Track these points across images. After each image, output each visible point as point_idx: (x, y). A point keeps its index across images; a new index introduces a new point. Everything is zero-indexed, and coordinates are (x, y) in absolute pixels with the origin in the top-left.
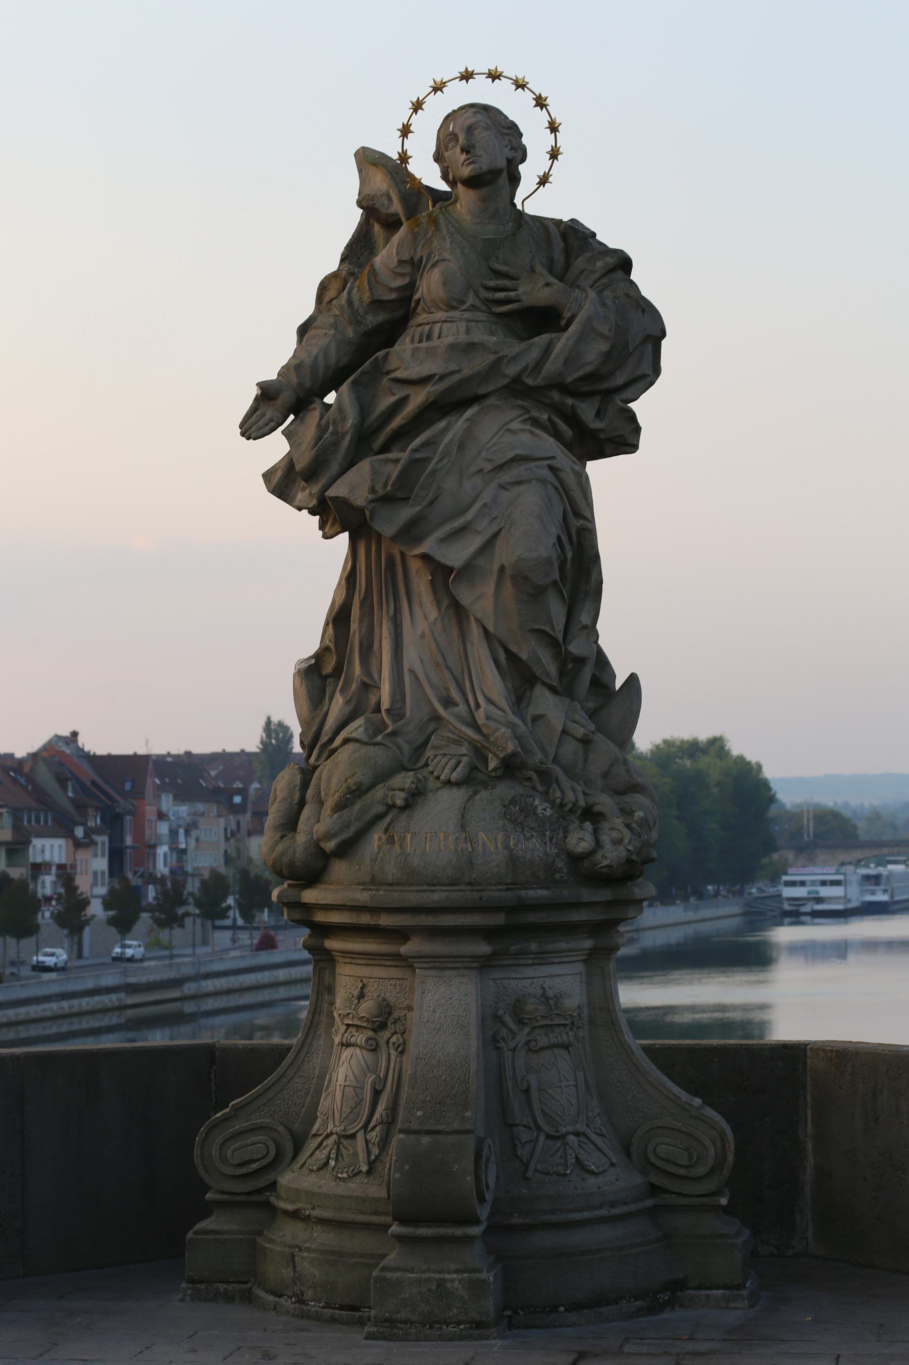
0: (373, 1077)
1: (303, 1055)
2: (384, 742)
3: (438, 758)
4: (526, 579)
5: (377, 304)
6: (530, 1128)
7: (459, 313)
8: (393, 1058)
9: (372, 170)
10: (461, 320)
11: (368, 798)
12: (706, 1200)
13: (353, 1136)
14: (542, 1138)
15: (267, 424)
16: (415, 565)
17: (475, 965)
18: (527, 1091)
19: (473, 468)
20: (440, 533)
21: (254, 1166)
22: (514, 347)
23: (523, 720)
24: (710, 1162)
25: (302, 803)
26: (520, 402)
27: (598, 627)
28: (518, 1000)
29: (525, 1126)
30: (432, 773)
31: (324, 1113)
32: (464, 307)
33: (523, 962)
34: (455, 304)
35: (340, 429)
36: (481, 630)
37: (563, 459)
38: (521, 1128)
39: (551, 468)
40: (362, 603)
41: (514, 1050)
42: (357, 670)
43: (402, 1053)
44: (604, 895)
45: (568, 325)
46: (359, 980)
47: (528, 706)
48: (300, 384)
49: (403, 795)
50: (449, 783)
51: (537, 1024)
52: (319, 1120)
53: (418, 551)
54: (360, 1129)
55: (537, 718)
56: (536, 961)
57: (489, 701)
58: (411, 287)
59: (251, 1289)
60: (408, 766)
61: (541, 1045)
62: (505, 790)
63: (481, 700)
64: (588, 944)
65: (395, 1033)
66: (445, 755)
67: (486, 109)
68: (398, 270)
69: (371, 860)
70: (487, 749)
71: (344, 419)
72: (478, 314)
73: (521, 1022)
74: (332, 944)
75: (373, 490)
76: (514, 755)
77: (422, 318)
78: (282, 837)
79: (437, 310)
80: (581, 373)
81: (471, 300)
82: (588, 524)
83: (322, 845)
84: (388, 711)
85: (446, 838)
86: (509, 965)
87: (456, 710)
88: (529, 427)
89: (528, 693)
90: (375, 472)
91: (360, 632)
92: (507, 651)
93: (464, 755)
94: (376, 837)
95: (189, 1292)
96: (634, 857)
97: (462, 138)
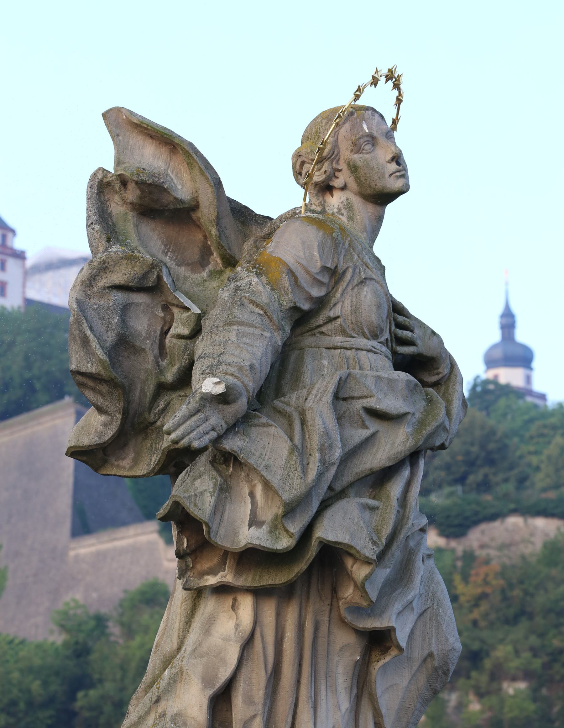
7: (377, 343)
15: (208, 433)
35: (327, 459)
68: (319, 277)
79: (358, 335)
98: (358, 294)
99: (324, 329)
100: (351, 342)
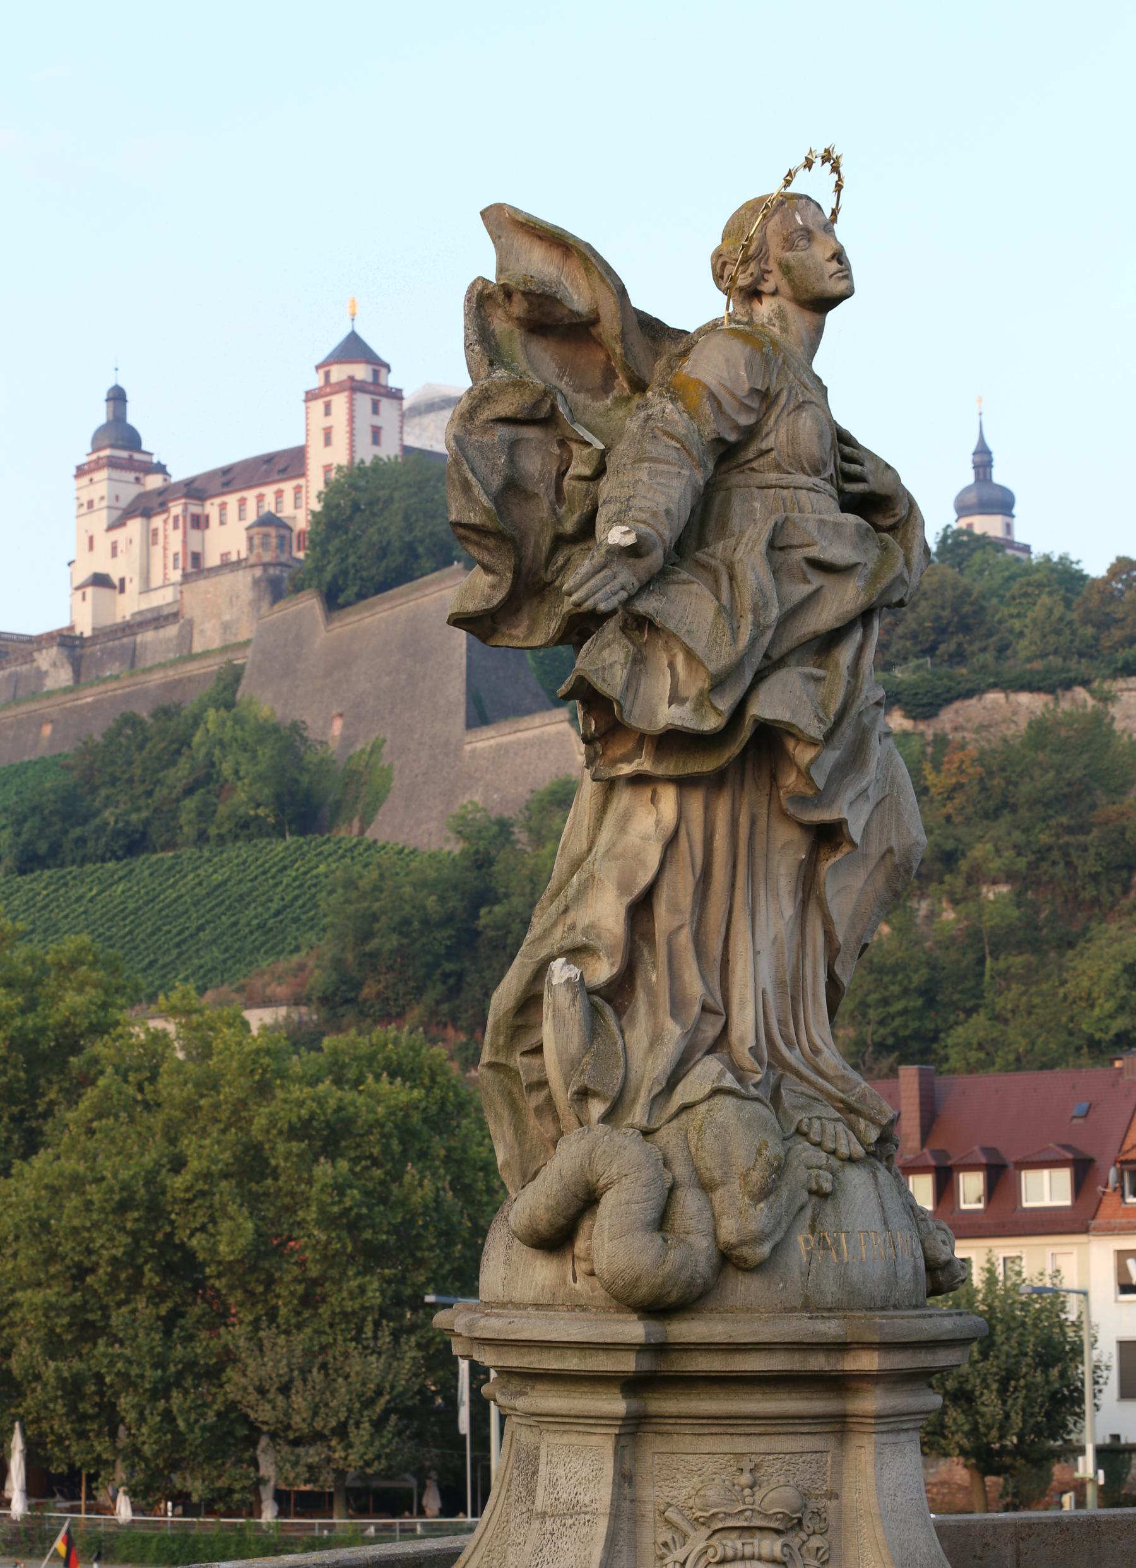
9: (522, 243)
15: (616, 593)
69: (802, 1274)
98: (795, 421)
99: (754, 465)
100: (787, 479)
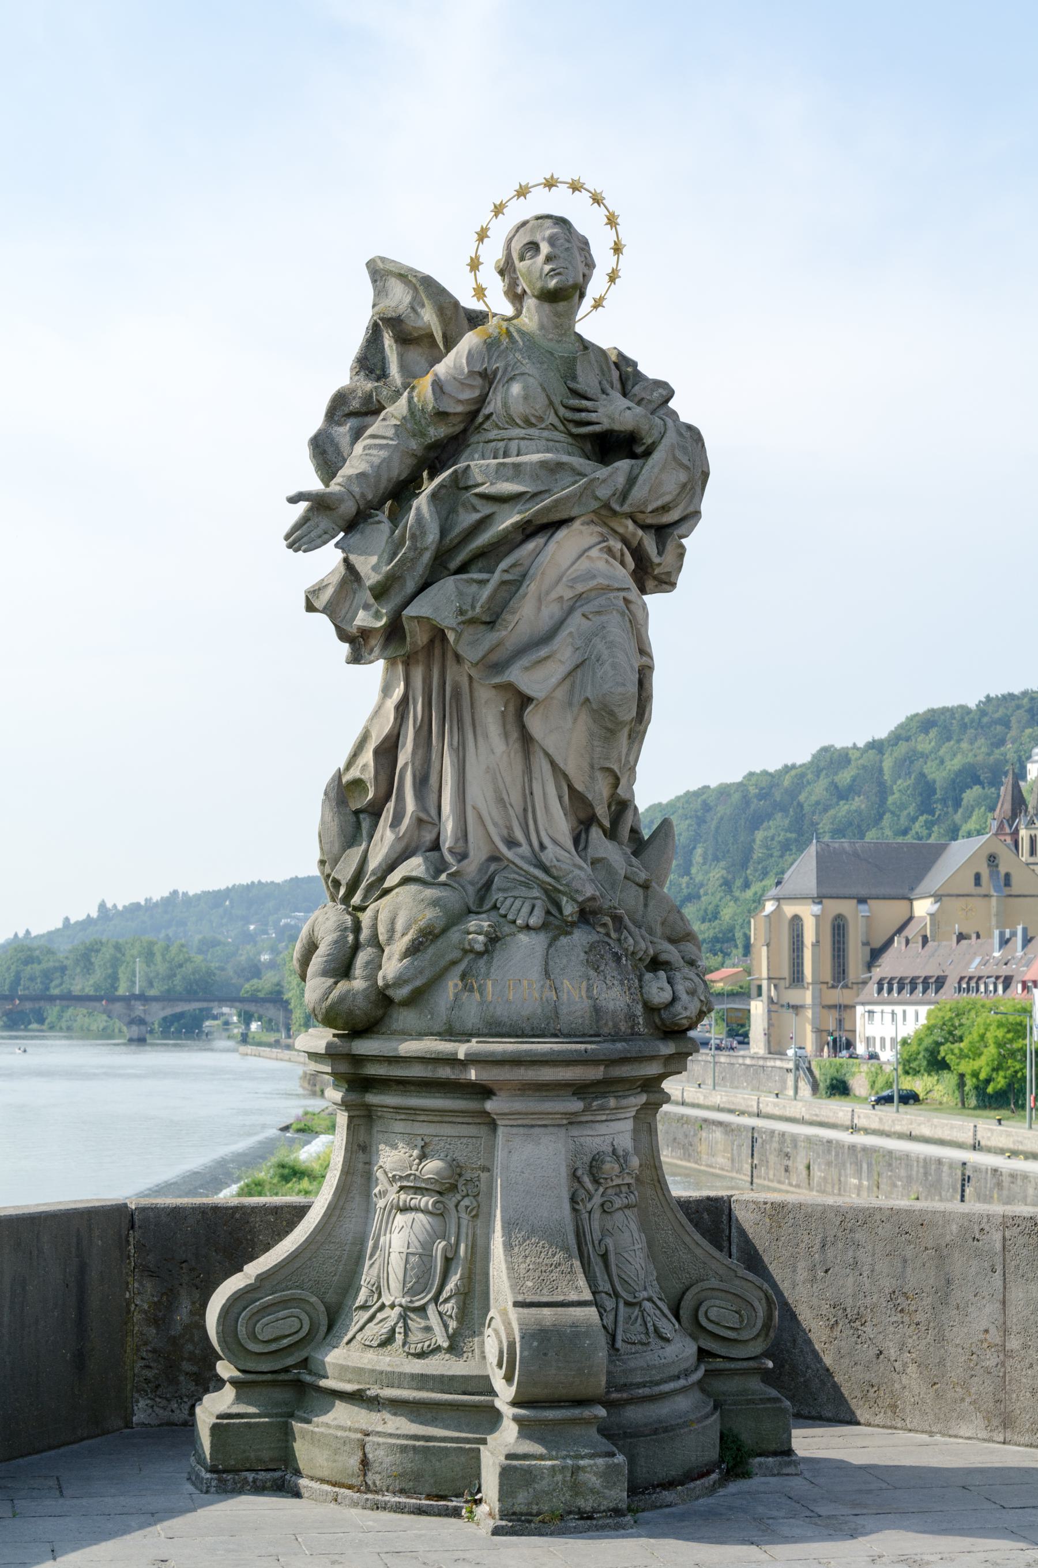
0: (444, 1243)
1: (334, 1219)
2: (449, 882)
3: (508, 902)
4: (612, 713)
5: (441, 415)
6: (610, 1295)
8: (464, 1222)
10: (540, 438)
11: (441, 943)
12: (752, 1364)
13: (422, 1310)
14: (621, 1305)
16: (485, 694)
17: (565, 1122)
18: (605, 1257)
19: (554, 595)
20: (525, 661)
21: (285, 1342)
22: (603, 472)
23: (585, 861)
24: (759, 1324)
25: (356, 947)
26: (599, 529)
27: (637, 768)
28: (593, 1159)
29: (606, 1293)
30: (505, 916)
31: (372, 1282)
32: (543, 426)
33: (599, 1118)
34: (533, 420)
35: (419, 545)
36: (549, 766)
37: (634, 593)
38: (603, 1295)
39: (625, 599)
40: (417, 733)
41: (590, 1212)
42: (410, 805)
43: (476, 1216)
44: (668, 1048)
45: (648, 453)
46: (419, 1138)
47: (586, 848)
48: (363, 495)
49: (481, 938)
50: (527, 927)
51: (611, 1184)
52: (363, 1289)
53: (498, 680)
54: (430, 1300)
55: (594, 862)
56: (609, 1117)
57: (555, 842)
58: (482, 400)
59: (283, 1477)
60: (474, 908)
61: (617, 1206)
62: (580, 938)
63: (546, 841)
64: (643, 1098)
65: (468, 1195)
66: (516, 898)
67: (562, 222)
70: (559, 891)
71: (424, 534)
72: (557, 433)
73: (596, 1181)
74: (372, 1099)
75: (461, 612)
76: (593, 899)
77: (493, 434)
78: (336, 983)
80: (659, 503)
81: (552, 419)
82: (649, 661)
83: (390, 992)
84: (451, 850)
85: (530, 985)
86: (587, 1122)
87: (520, 850)
88: (606, 556)
89: (583, 836)
90: (461, 594)
91: (413, 764)
92: (570, 787)
93: (536, 898)
94: (452, 984)
95: (214, 1483)
96: (705, 1009)
97: (545, 249)
98: (508, 389)
99: (485, 426)
